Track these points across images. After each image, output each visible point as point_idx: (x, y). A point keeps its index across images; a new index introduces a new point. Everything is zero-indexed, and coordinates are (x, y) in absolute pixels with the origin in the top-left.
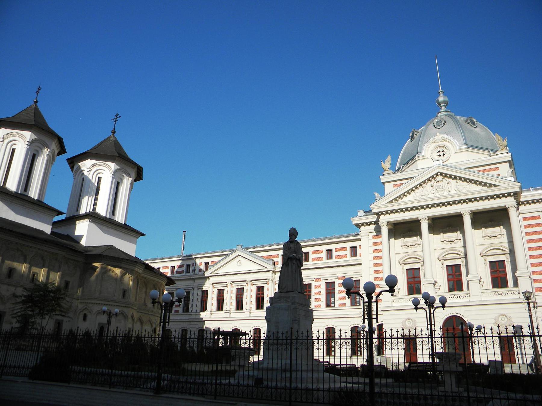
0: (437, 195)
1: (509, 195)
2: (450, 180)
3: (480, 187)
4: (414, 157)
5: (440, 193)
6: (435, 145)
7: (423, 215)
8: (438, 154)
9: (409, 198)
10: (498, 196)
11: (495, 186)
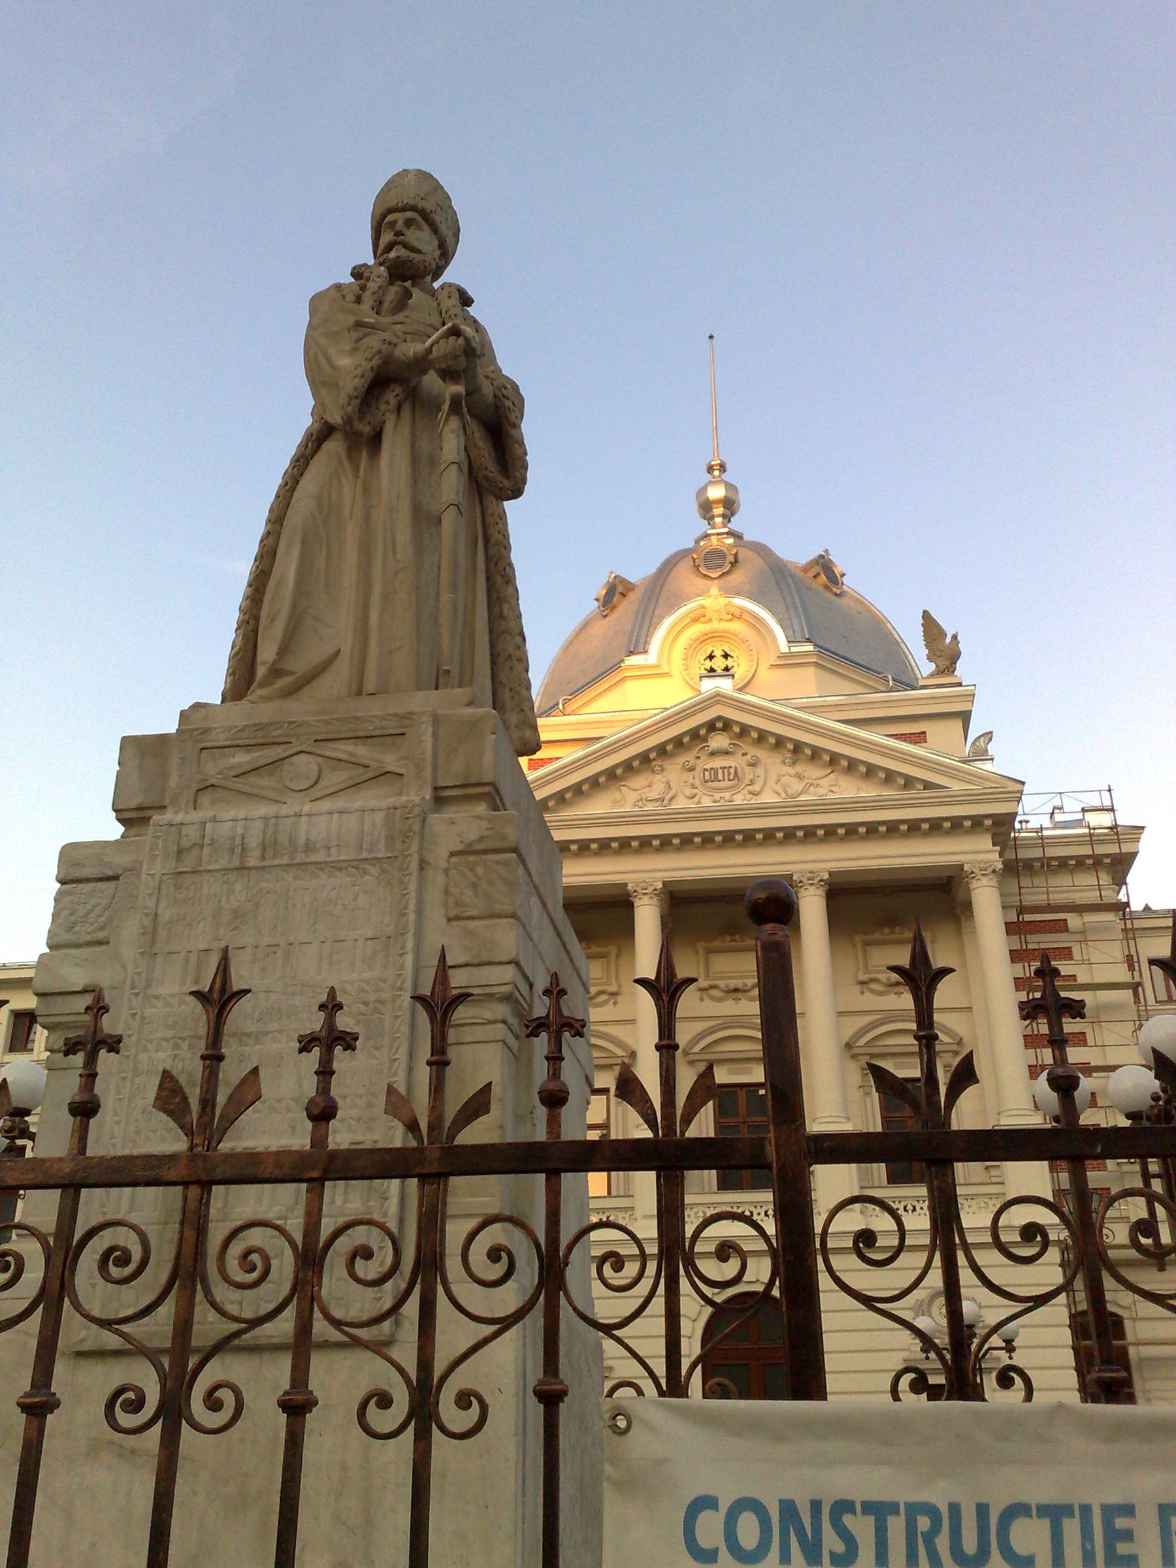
0: (707, 802)
1: (977, 823)
2: (762, 754)
3: (868, 791)
4: (616, 666)
5: (717, 796)
6: (697, 629)
7: (646, 875)
8: (708, 664)
9: (598, 806)
10: (935, 827)
11: (928, 786)
